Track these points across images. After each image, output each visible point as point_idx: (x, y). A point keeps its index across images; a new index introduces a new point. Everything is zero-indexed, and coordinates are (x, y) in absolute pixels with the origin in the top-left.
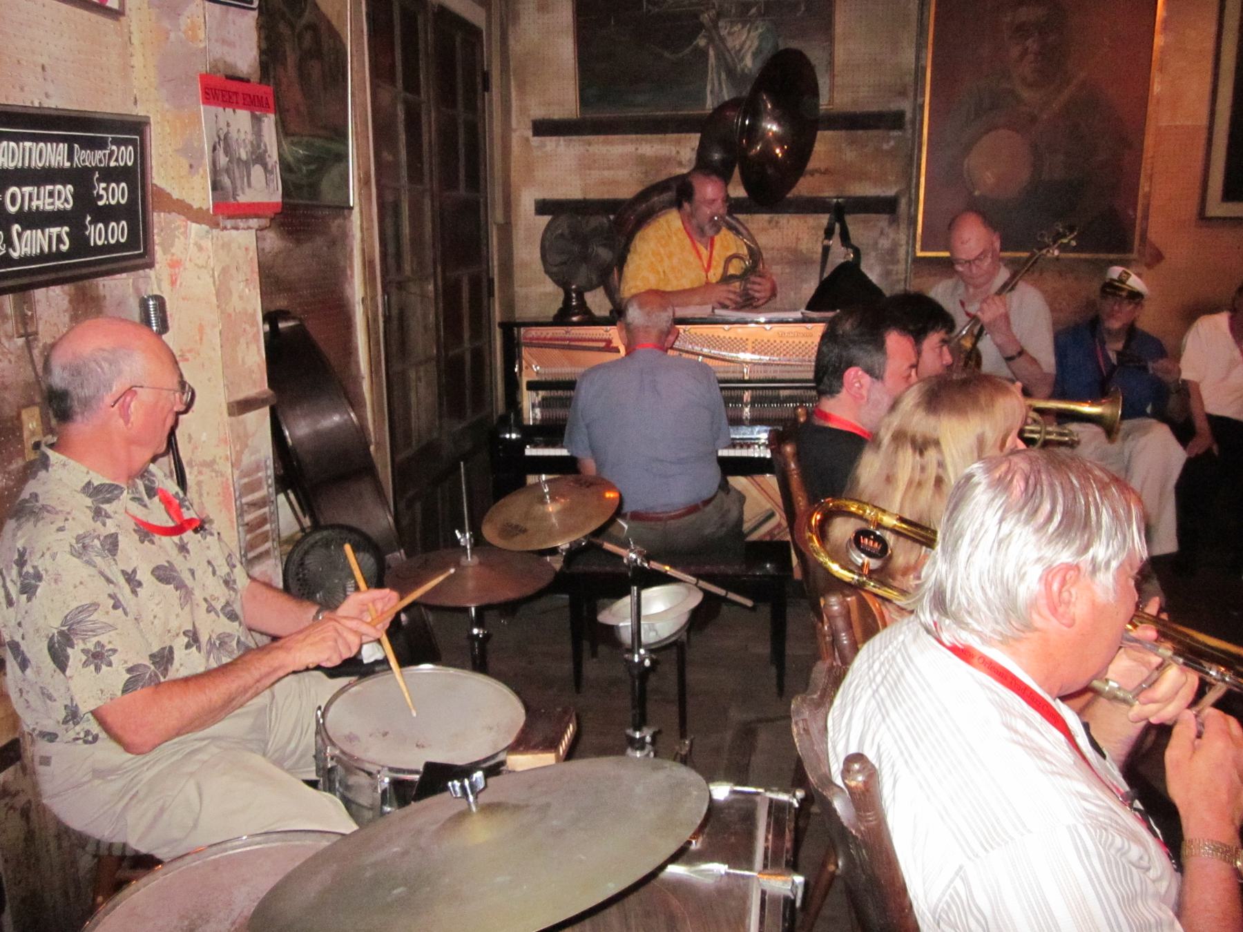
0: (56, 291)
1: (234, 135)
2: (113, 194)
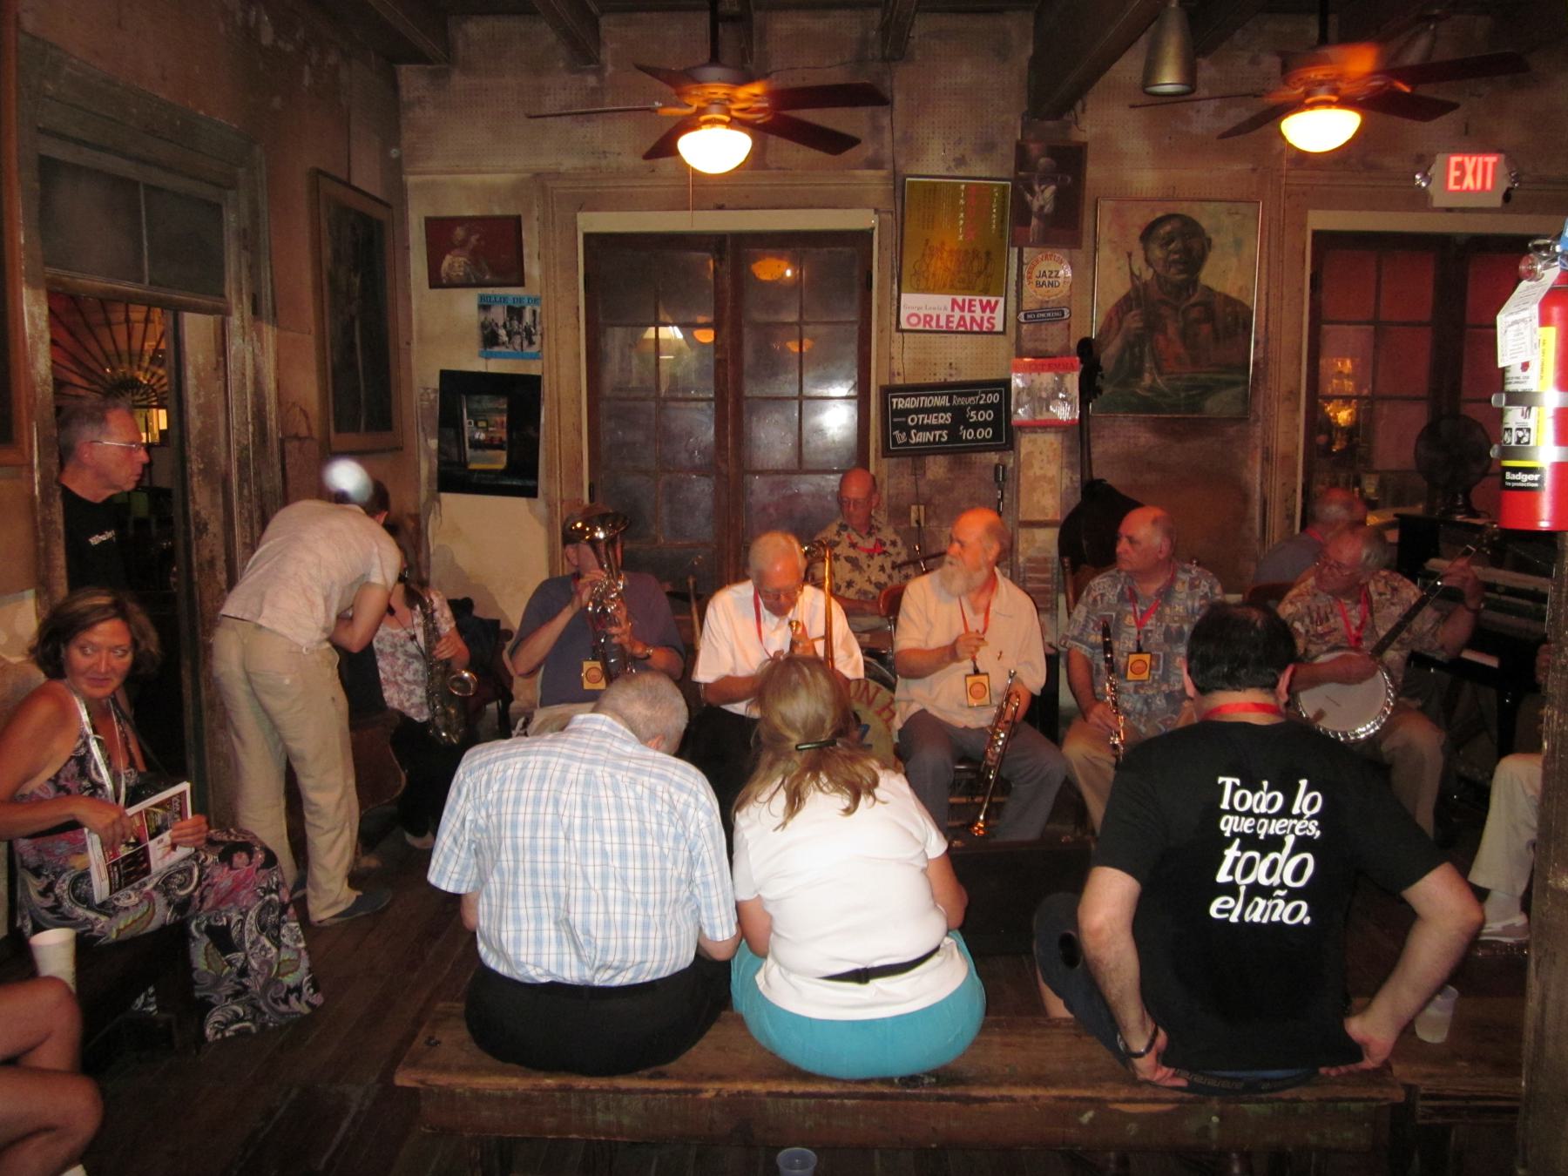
0: (941, 459)
1: (1037, 383)
2: (988, 416)
